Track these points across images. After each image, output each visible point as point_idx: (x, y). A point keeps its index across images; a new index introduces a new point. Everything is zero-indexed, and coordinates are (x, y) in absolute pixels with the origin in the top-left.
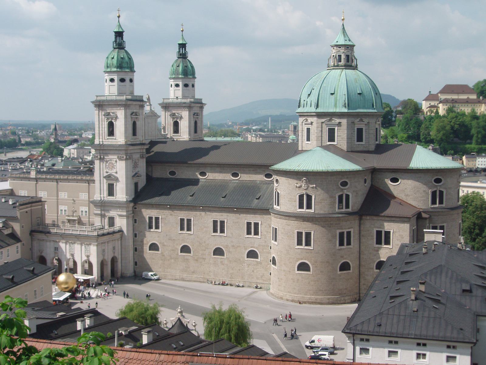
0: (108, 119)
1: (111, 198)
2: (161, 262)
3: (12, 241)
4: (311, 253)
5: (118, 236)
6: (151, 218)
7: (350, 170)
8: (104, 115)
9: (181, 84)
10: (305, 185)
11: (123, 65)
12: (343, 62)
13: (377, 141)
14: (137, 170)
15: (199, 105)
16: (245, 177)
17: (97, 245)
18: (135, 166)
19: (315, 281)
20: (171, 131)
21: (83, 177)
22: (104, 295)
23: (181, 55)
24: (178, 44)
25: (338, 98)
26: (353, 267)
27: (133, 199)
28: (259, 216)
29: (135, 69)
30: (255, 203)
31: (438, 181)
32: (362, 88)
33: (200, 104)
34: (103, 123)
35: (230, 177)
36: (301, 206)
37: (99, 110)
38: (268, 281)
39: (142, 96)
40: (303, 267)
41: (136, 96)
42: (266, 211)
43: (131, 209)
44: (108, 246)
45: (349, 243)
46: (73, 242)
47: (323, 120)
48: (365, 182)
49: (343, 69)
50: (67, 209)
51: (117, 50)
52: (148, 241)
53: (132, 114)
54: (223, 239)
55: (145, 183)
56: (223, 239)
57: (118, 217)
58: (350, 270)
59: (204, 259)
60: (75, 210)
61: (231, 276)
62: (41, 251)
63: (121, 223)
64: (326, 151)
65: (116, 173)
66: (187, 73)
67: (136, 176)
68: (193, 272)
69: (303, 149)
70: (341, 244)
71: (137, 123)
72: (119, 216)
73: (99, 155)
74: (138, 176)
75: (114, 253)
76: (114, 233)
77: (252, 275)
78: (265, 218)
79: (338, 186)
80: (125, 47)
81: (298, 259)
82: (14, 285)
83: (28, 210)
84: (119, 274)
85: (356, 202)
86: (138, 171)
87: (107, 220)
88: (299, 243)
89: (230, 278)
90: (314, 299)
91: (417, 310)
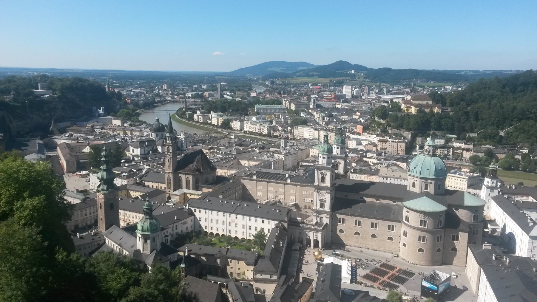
0: (322, 175)
1: (322, 209)
12: (431, 153)
57: (325, 218)
59: (367, 238)
87: (319, 218)
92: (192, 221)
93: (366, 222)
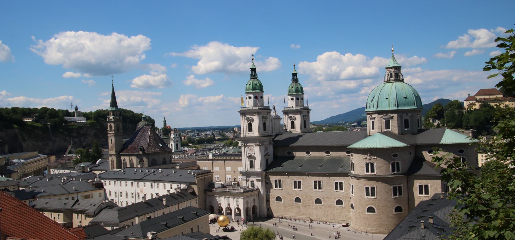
0: (248, 121)
1: (252, 170)
2: (283, 208)
3: (193, 196)
4: (375, 200)
5: (256, 192)
6: (276, 181)
7: (399, 147)
8: (246, 119)
10: (369, 157)
11: (256, 88)
12: (393, 78)
13: (419, 127)
14: (267, 152)
15: (307, 110)
16: (333, 154)
17: (243, 199)
18: (266, 149)
19: (379, 219)
20: (290, 128)
21: (240, 157)
23: (294, 80)
24: (292, 74)
25: (391, 101)
26: (404, 209)
27: (265, 169)
29: (264, 90)
30: (340, 169)
31: (461, 151)
32: (406, 93)
33: (307, 110)
34: (246, 124)
35: (324, 154)
36: (367, 171)
38: (350, 219)
39: (269, 107)
40: (371, 210)
41: (265, 107)
42: (346, 175)
43: (264, 176)
44: (250, 198)
45: (400, 194)
46: (229, 197)
47: (382, 116)
48: (410, 154)
49: (394, 82)
50: (230, 177)
51: (252, 79)
52: (275, 195)
53: (262, 118)
55: (273, 159)
57: (256, 180)
58: (402, 211)
59: (310, 206)
60: (235, 178)
61: (327, 216)
62: (211, 202)
63: (258, 185)
64: (383, 135)
67: (267, 155)
68: (303, 214)
69: (370, 135)
70: (395, 194)
71: (266, 123)
72: (257, 180)
73: (243, 143)
74: (268, 156)
75: (254, 203)
76: (254, 190)
77: (339, 216)
78: (346, 179)
79: (391, 157)
80: (257, 78)
81: (367, 205)
82: (184, 222)
83: (203, 178)
84: (258, 216)
85: (404, 166)
86: (268, 153)
87: (249, 182)
88: (367, 194)
89: (326, 218)
90: (379, 230)
91: (425, 235)
92: (100, 196)
93: (308, 182)
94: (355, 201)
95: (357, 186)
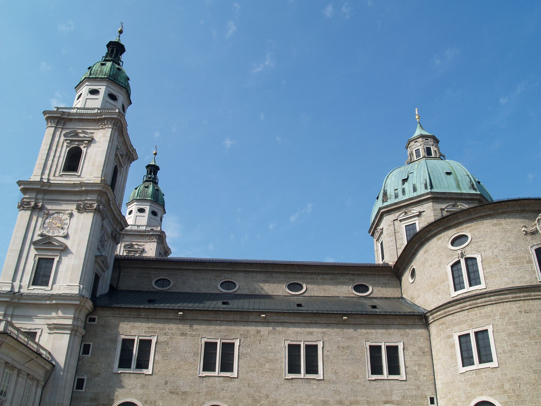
1: (39, 290)
9: (147, 209)
11: (119, 78)
22: (213, 332)
25: (459, 178)
28: (397, 331)
34: (59, 149)
35: (284, 290)
37: (56, 128)
47: (443, 206)
54: (315, 387)
56: (315, 387)
65: (66, 237)
66: (158, 199)
94: (507, 386)
95: (516, 323)
